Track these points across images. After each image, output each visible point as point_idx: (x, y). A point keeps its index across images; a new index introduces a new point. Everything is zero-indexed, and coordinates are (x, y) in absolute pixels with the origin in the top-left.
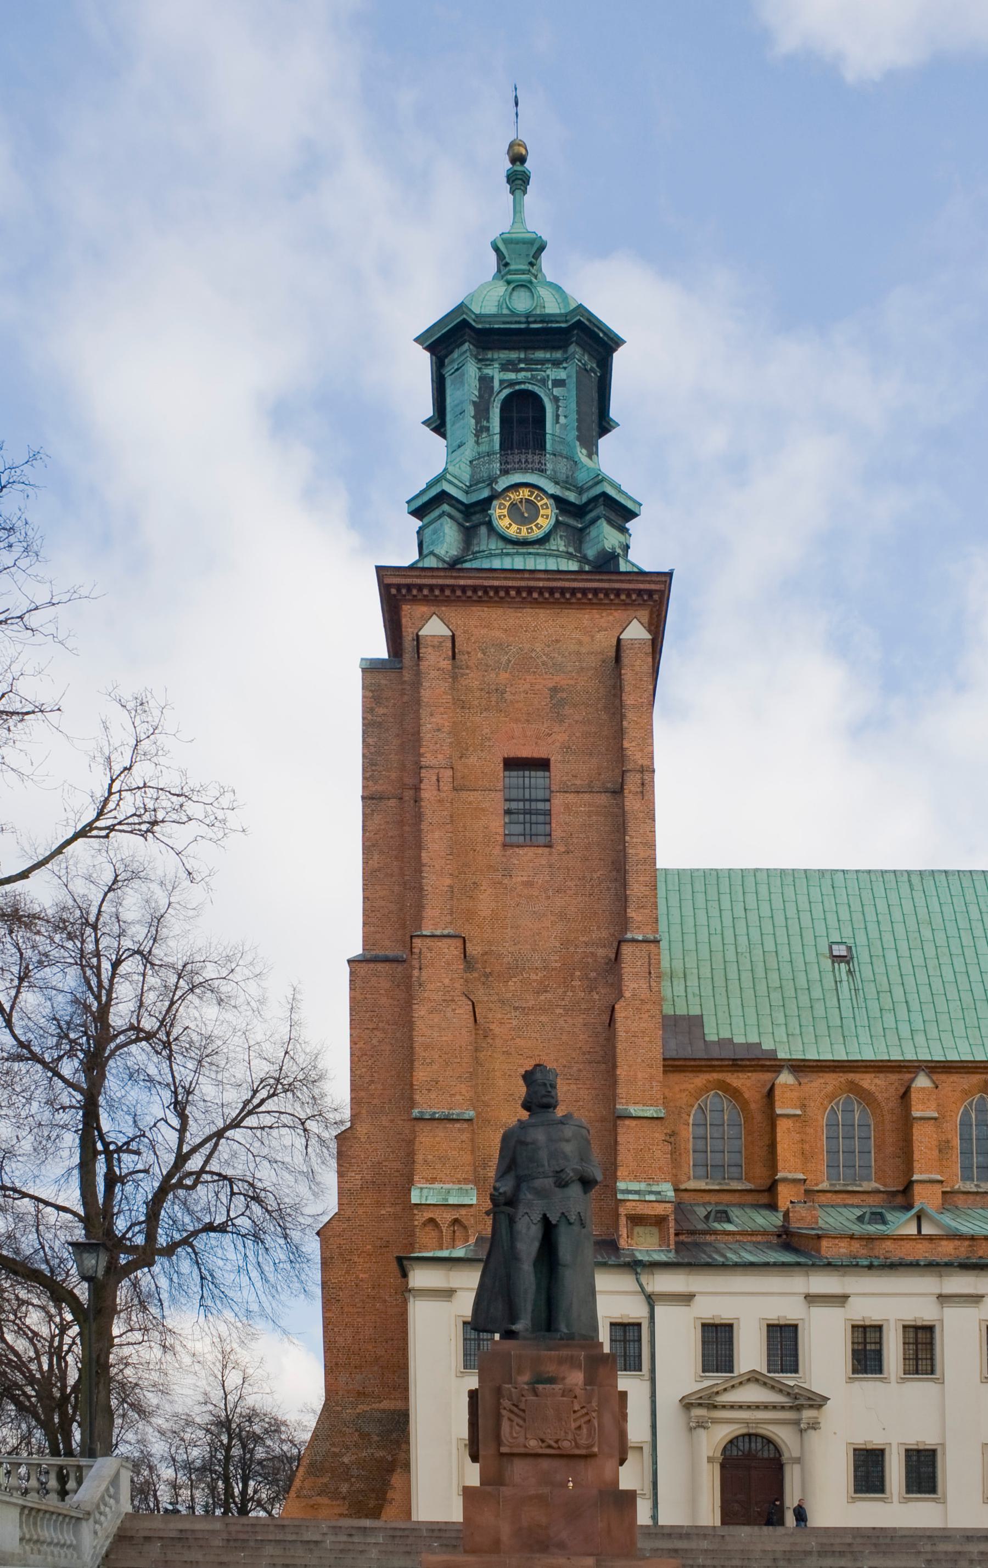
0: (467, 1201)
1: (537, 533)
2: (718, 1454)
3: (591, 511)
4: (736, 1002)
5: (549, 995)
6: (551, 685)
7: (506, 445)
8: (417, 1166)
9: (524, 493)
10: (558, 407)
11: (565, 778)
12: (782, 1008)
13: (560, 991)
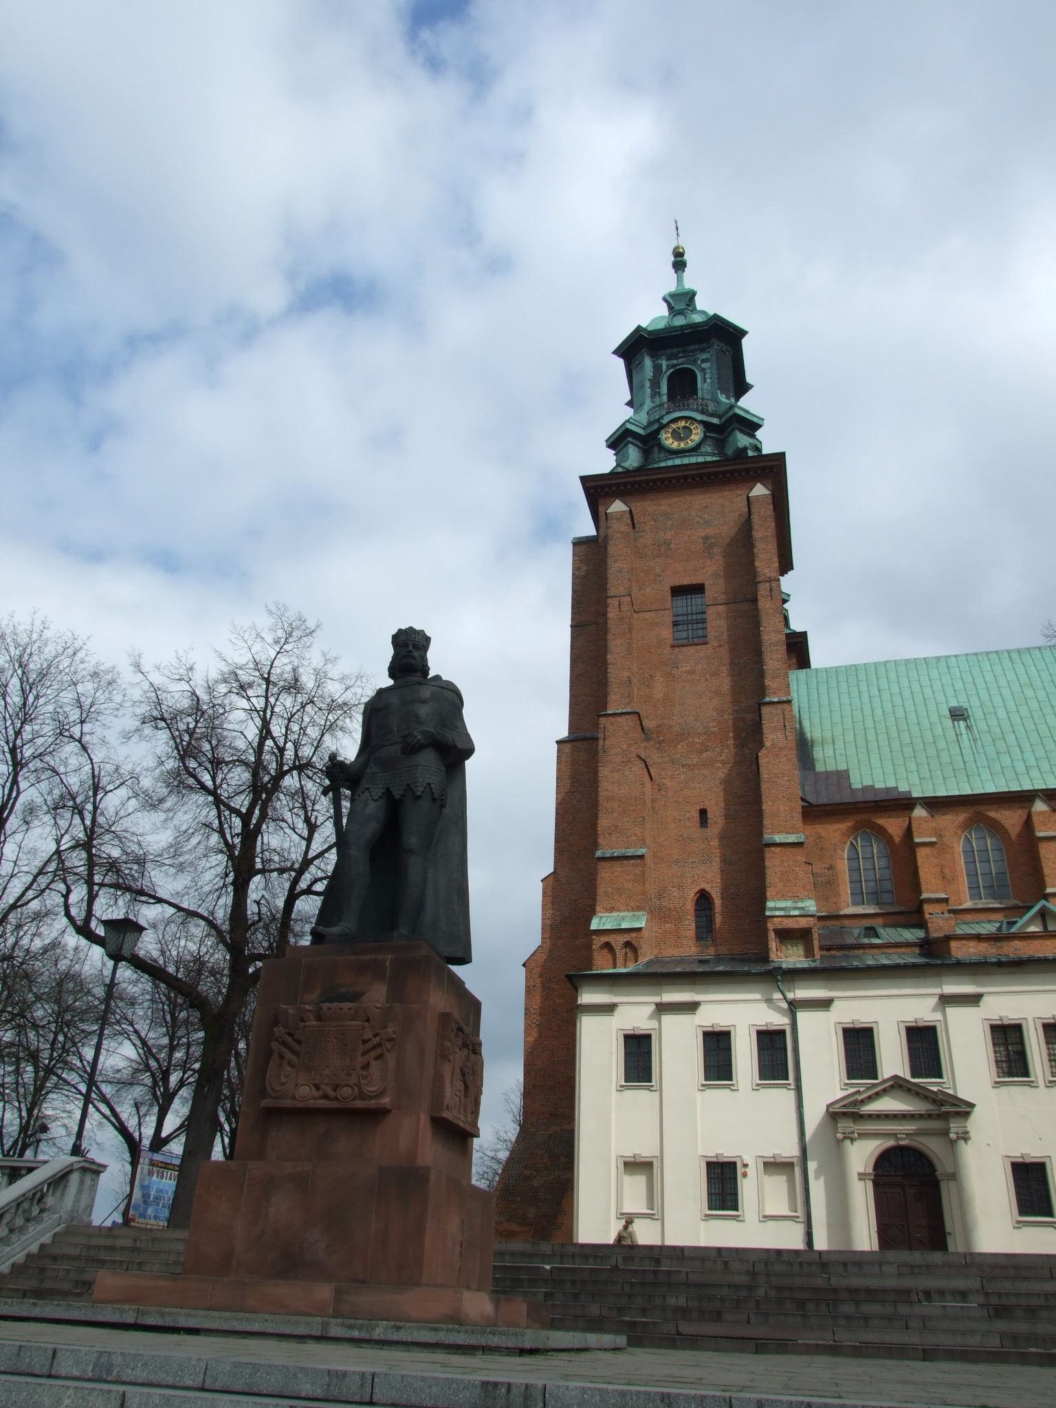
0: (637, 925)
1: (691, 444)
2: (870, 1170)
3: (729, 427)
4: (875, 758)
5: (709, 754)
6: (702, 535)
7: (671, 396)
8: (599, 898)
9: (683, 423)
10: (705, 374)
11: (716, 595)
12: (913, 759)
13: (718, 750)
